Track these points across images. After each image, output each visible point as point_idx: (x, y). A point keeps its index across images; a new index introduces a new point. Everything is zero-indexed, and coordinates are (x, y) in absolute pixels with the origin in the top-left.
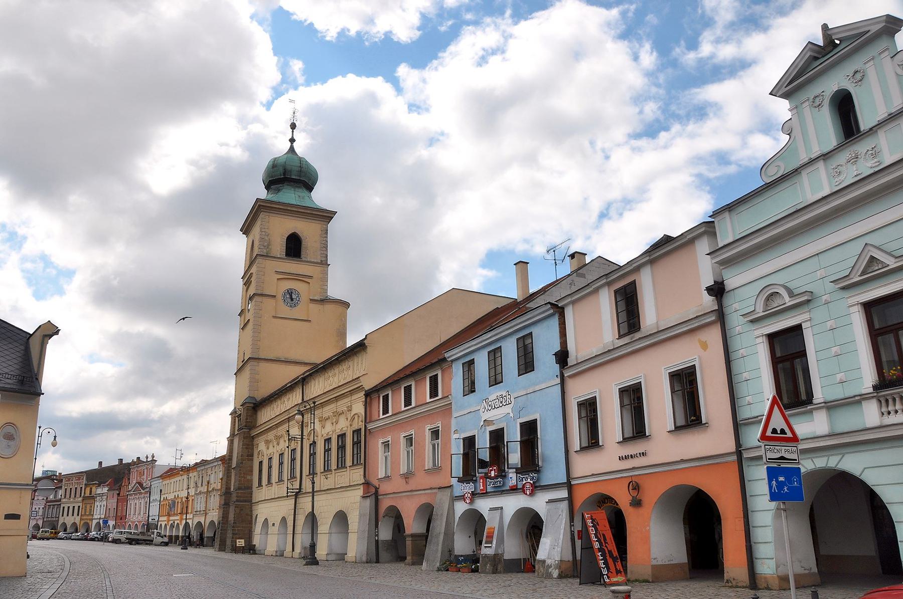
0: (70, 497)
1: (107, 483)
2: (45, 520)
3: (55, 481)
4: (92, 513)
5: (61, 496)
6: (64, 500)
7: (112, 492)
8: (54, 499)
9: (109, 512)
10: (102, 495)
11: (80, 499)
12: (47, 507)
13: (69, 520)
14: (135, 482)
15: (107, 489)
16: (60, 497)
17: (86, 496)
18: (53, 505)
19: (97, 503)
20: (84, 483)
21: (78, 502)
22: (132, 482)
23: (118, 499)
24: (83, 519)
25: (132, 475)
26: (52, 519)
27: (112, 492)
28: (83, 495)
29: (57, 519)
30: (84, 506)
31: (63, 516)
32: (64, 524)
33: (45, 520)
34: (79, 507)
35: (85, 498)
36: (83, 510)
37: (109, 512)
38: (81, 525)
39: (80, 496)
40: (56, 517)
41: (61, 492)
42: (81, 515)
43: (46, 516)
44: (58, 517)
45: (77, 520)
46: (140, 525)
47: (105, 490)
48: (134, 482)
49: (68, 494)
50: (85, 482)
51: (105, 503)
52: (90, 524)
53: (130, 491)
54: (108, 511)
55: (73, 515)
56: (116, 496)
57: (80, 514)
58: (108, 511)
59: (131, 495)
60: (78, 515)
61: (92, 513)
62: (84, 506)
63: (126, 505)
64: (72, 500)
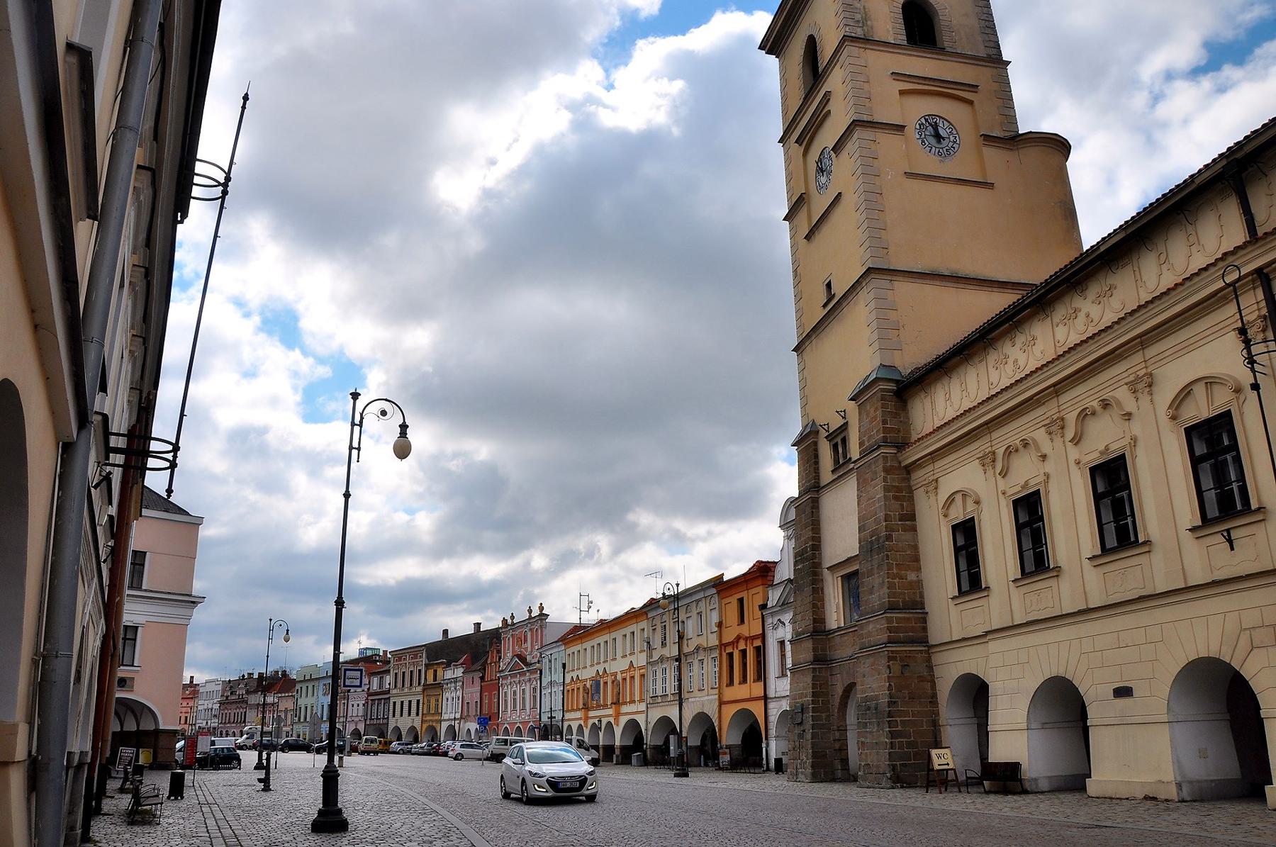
0: (403, 686)
1: (461, 661)
2: (368, 722)
3: (378, 664)
4: (440, 711)
5: (389, 684)
6: (394, 691)
7: (471, 675)
9: (468, 708)
10: (455, 680)
11: (419, 689)
12: (370, 702)
13: (404, 723)
14: (510, 655)
15: (462, 670)
18: (378, 699)
19: (447, 695)
20: (424, 663)
21: (415, 695)
22: (505, 654)
24: (426, 721)
25: (505, 644)
26: (378, 722)
27: (470, 676)
28: (423, 682)
29: (385, 721)
30: (426, 700)
31: (394, 716)
32: (397, 729)
33: (368, 722)
34: (418, 701)
35: (426, 687)
36: (425, 706)
37: (468, 708)
38: (424, 729)
39: (419, 684)
41: (388, 679)
42: (423, 714)
43: (369, 717)
44: (388, 718)
45: (417, 723)
46: (525, 729)
47: (459, 672)
48: (508, 656)
49: (400, 681)
50: (424, 660)
51: (459, 693)
52: (438, 730)
53: (502, 671)
54: (465, 707)
55: (409, 715)
56: (477, 681)
57: (420, 713)
58: (465, 707)
59: (505, 678)
60: (418, 714)
61: (440, 711)
62: (426, 700)
63: (496, 696)
64: (406, 690)
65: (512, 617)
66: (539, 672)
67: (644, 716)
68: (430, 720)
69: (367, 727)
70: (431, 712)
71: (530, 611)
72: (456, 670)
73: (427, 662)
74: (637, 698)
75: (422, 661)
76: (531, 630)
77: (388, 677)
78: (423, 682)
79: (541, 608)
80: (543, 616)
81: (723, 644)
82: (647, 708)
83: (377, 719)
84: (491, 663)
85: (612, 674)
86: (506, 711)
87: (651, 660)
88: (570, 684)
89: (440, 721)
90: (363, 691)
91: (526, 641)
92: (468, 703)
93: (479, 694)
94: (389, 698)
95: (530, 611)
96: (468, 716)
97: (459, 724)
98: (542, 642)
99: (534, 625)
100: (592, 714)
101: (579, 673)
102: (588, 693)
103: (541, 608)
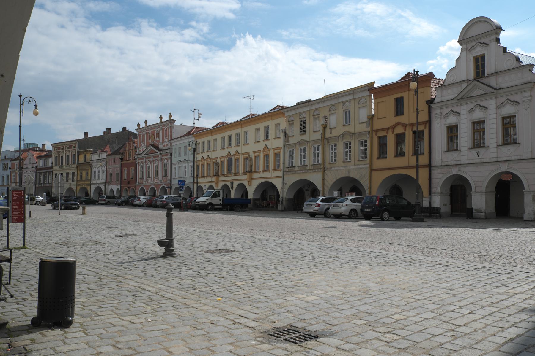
0: (62, 164)
2: (37, 186)
4: (90, 179)
5: (52, 163)
6: (56, 167)
8: (44, 167)
16: (50, 165)
17: (80, 162)
20: (77, 150)
23: (121, 163)
28: (76, 161)
30: (79, 172)
33: (37, 186)
34: (73, 173)
40: (49, 183)
42: (77, 181)
60: (73, 181)
62: (79, 172)
65: (146, 122)
66: (169, 155)
67: (280, 180)
68: (83, 184)
69: (36, 188)
70: (83, 179)
71: (161, 118)
72: (101, 155)
73: (79, 150)
74: (272, 166)
75: (75, 150)
76: (162, 129)
77: (50, 160)
78: (76, 161)
79: (170, 116)
80: (171, 121)
81: (375, 131)
82: (284, 174)
83: (44, 183)
84: (128, 150)
85: (244, 154)
86: (142, 177)
87: (287, 144)
88: (201, 160)
89: (90, 185)
90: (33, 167)
91: (157, 136)
92: (111, 174)
93: (119, 169)
94: (52, 171)
95: (161, 118)
96: (111, 181)
97: (105, 186)
98: (171, 136)
99: (164, 126)
100: (221, 179)
101: (209, 154)
102: (219, 167)
103: (170, 116)
